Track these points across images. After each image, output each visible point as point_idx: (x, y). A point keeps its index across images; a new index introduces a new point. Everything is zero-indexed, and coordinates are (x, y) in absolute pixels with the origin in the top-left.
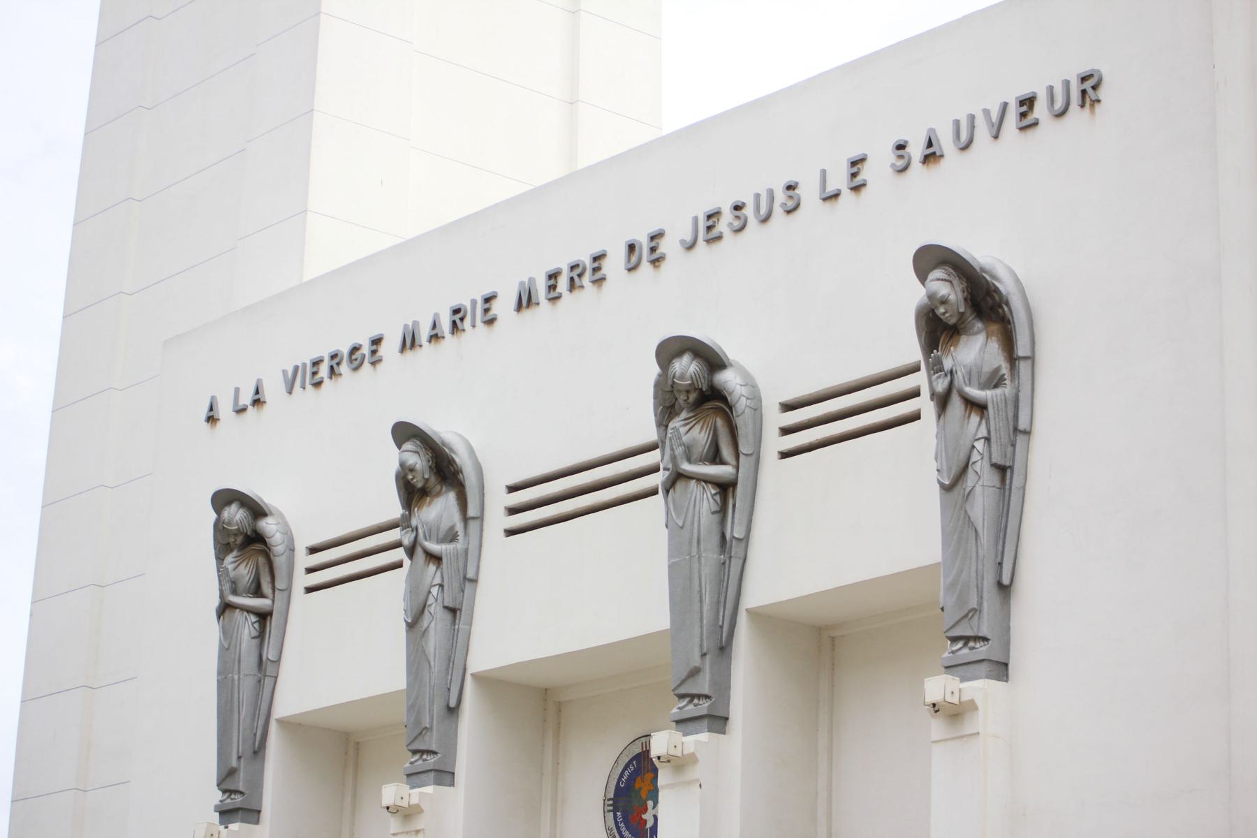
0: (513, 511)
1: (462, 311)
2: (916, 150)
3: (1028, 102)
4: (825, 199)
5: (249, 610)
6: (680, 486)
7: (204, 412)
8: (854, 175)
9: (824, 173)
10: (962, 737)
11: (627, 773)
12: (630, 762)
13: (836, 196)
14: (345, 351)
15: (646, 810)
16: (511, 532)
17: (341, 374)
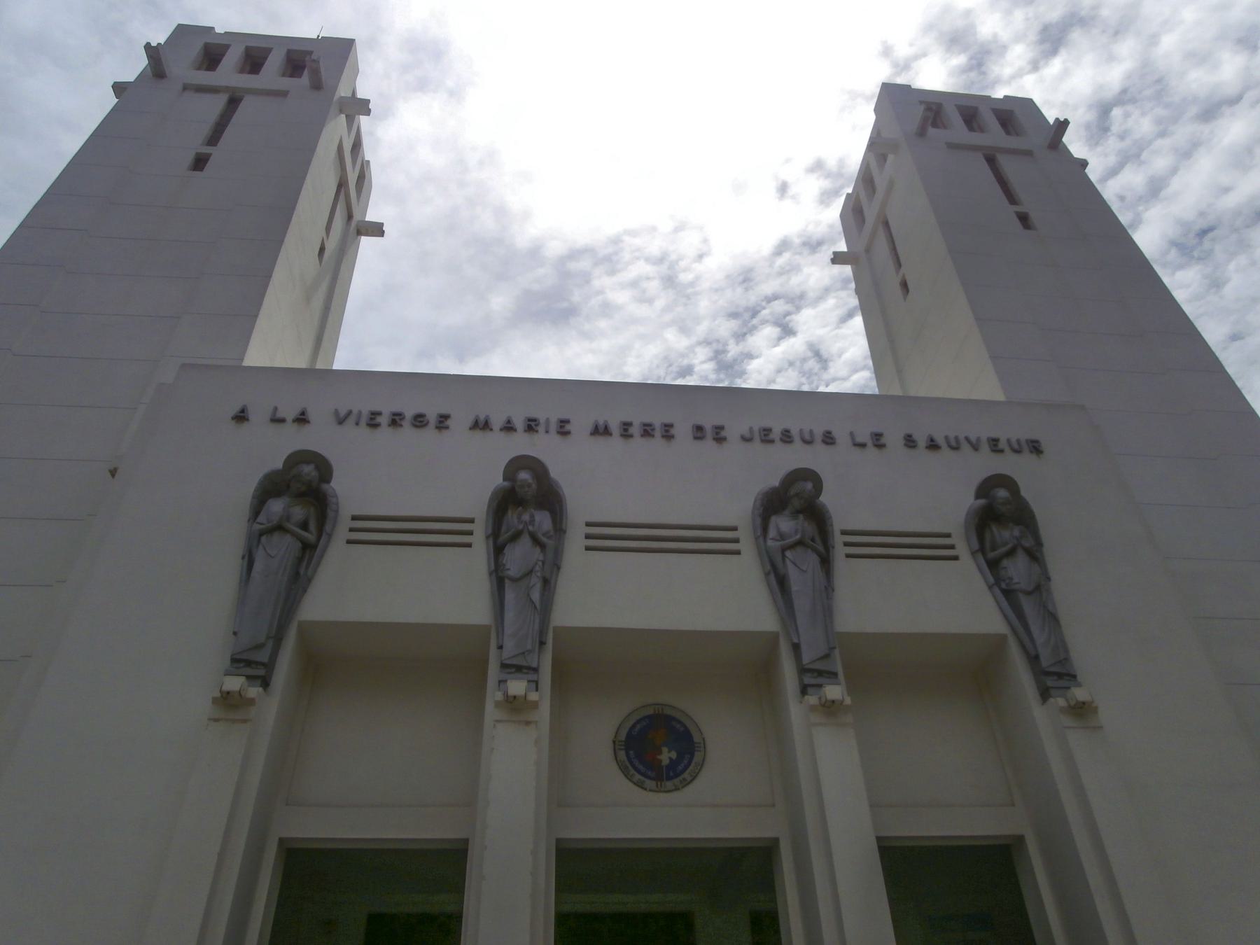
0: (588, 537)
1: (537, 422)
2: (922, 443)
5: (293, 534)
7: (235, 409)
9: (852, 434)
11: (638, 727)
12: (638, 722)
14: (409, 414)
15: (660, 753)
16: (588, 548)
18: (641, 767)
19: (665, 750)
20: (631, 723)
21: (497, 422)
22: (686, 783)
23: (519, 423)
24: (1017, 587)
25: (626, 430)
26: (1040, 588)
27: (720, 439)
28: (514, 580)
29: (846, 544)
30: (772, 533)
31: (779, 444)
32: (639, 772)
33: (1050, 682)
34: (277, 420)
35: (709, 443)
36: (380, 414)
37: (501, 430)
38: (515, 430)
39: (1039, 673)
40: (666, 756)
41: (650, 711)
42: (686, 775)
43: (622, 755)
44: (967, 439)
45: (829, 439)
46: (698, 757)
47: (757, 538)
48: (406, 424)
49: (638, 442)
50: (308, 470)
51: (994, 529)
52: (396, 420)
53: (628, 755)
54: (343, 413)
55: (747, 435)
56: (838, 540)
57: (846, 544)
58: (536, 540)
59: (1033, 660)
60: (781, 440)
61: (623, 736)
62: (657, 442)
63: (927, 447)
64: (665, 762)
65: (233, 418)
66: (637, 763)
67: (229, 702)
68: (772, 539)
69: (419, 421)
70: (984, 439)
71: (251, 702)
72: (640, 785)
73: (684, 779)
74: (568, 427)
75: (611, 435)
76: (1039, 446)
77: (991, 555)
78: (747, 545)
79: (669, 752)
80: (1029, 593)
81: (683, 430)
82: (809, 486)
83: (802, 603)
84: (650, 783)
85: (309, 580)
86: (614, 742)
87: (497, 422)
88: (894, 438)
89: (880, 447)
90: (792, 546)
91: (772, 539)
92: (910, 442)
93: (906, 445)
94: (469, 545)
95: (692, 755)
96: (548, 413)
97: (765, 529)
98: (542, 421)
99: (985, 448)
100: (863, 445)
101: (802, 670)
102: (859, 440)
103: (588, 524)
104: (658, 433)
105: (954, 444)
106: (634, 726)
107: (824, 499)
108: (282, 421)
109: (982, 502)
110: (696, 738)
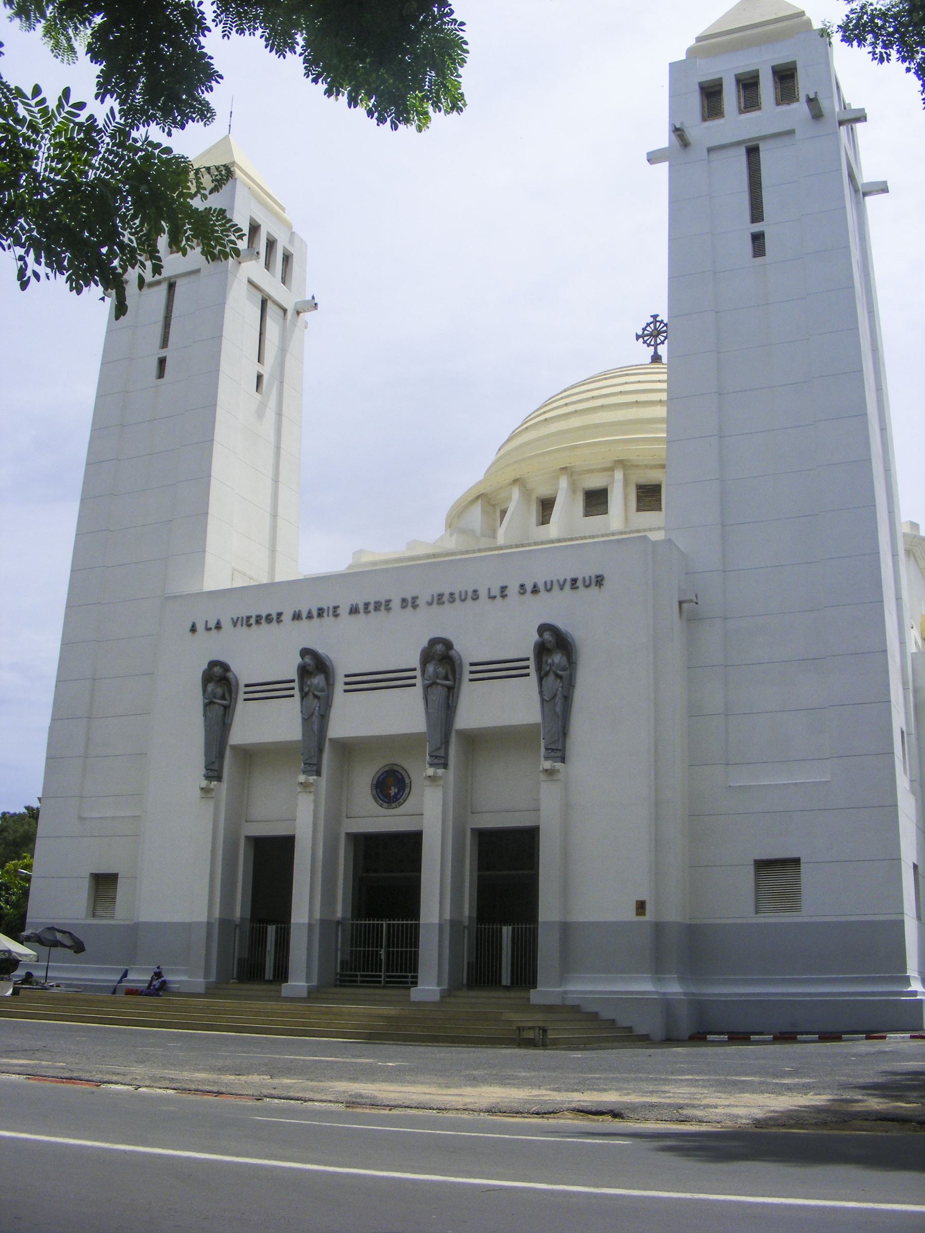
0: (346, 684)
2: (529, 588)
3: (574, 581)
5: (219, 704)
6: (434, 686)
7: (189, 627)
8: (502, 592)
10: (554, 780)
11: (382, 776)
12: (382, 774)
13: (494, 597)
15: (391, 790)
16: (346, 691)
18: (382, 797)
19: (393, 788)
20: (379, 775)
23: (315, 613)
27: (415, 606)
29: (471, 672)
32: (382, 800)
34: (208, 629)
36: (251, 617)
40: (393, 791)
42: (401, 800)
44: (558, 581)
46: (407, 791)
48: (263, 621)
49: (373, 614)
50: (217, 669)
53: (377, 791)
58: (316, 696)
62: (383, 612)
64: (393, 794)
66: (380, 795)
67: (205, 791)
69: (269, 619)
71: (212, 790)
72: (381, 806)
75: (359, 613)
81: (396, 604)
84: (386, 805)
87: (304, 615)
95: (404, 790)
96: (327, 603)
98: (326, 608)
99: (568, 585)
102: (493, 594)
103: (346, 676)
104: (382, 608)
106: (380, 777)
110: (407, 781)
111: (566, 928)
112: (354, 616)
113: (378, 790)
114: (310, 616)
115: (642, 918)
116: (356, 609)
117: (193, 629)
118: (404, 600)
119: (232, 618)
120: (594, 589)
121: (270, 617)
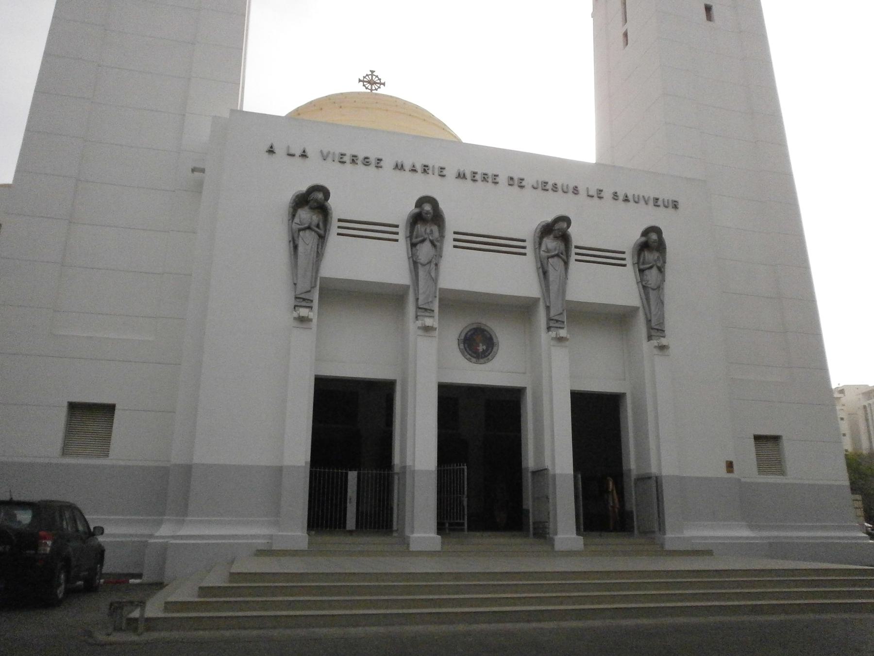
0: (455, 240)
2: (621, 198)
4: (588, 196)
7: (267, 147)
9: (588, 188)
11: (469, 334)
14: (361, 157)
15: (479, 347)
16: (455, 247)
17: (357, 164)
18: (470, 352)
19: (481, 344)
21: (408, 167)
22: (489, 360)
23: (419, 167)
24: (649, 286)
25: (474, 177)
26: (659, 288)
28: (423, 265)
29: (577, 254)
30: (543, 248)
31: (550, 192)
32: (470, 354)
33: (653, 333)
35: (515, 188)
37: (410, 171)
38: (417, 172)
39: (650, 328)
40: (481, 348)
41: (475, 326)
42: (490, 357)
43: (462, 346)
44: (643, 197)
45: (576, 191)
46: (495, 349)
47: (535, 249)
49: (480, 184)
50: (320, 196)
51: (646, 252)
52: (354, 160)
53: (464, 346)
54: (325, 154)
55: (535, 186)
56: (574, 251)
57: (577, 254)
59: (649, 321)
60: (552, 189)
61: (462, 338)
62: (490, 185)
63: (623, 201)
65: (267, 152)
68: (543, 251)
69: (366, 162)
70: (652, 197)
72: (469, 360)
73: (488, 359)
74: (444, 173)
76: (678, 205)
77: (642, 267)
78: (529, 251)
79: (483, 346)
80: (653, 289)
82: (565, 225)
83: (554, 288)
84: (474, 360)
85: (323, 254)
86: (458, 340)
87: (408, 167)
88: (607, 194)
89: (600, 198)
90: (553, 257)
91: (543, 251)
92: (615, 196)
93: (613, 198)
94: (397, 240)
95: (492, 349)
96: (434, 162)
97: (540, 244)
98: (431, 166)
99: (651, 203)
100: (592, 197)
101: (549, 319)
102: (590, 193)
103: (455, 233)
104: (490, 180)
105: (636, 200)
106: (467, 334)
107: (570, 230)
108: (293, 155)
109: (643, 239)
110: (495, 341)
111: (644, 479)
112: (460, 181)
113: (466, 345)
114: (414, 170)
115: (730, 475)
116: (464, 174)
117: (271, 151)
118: (512, 179)
119: (321, 152)
120: (671, 210)
121: (367, 160)
